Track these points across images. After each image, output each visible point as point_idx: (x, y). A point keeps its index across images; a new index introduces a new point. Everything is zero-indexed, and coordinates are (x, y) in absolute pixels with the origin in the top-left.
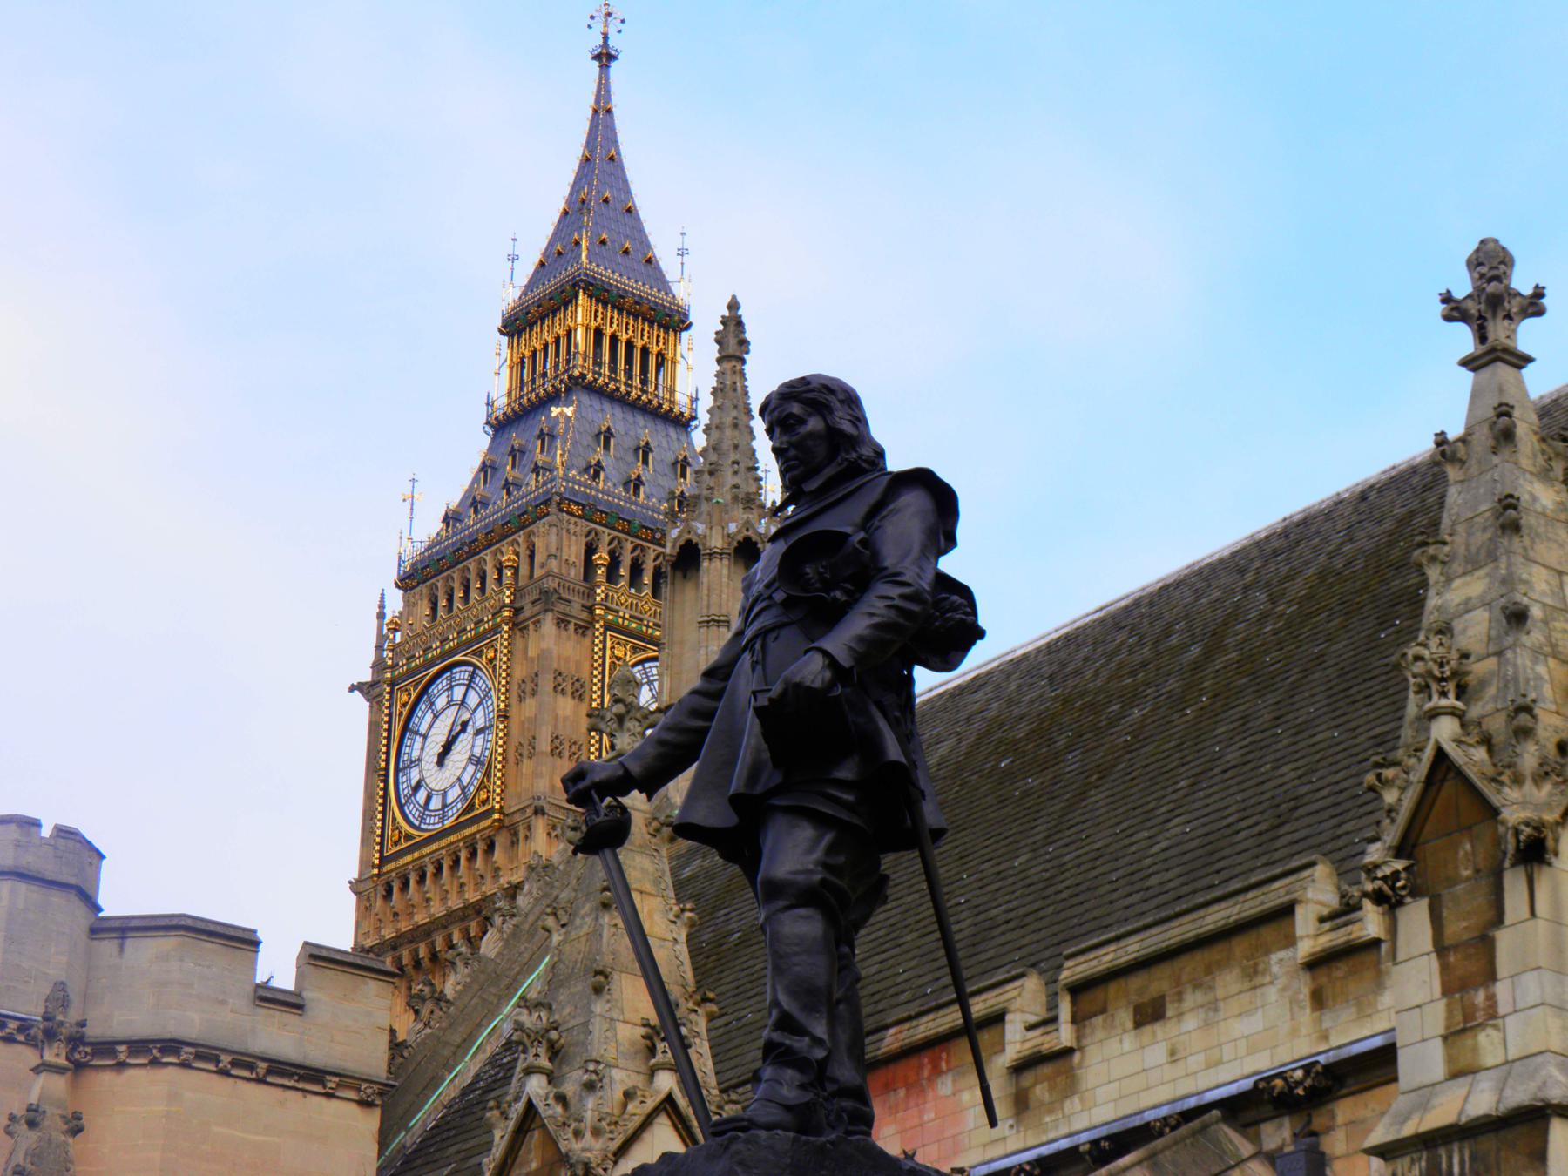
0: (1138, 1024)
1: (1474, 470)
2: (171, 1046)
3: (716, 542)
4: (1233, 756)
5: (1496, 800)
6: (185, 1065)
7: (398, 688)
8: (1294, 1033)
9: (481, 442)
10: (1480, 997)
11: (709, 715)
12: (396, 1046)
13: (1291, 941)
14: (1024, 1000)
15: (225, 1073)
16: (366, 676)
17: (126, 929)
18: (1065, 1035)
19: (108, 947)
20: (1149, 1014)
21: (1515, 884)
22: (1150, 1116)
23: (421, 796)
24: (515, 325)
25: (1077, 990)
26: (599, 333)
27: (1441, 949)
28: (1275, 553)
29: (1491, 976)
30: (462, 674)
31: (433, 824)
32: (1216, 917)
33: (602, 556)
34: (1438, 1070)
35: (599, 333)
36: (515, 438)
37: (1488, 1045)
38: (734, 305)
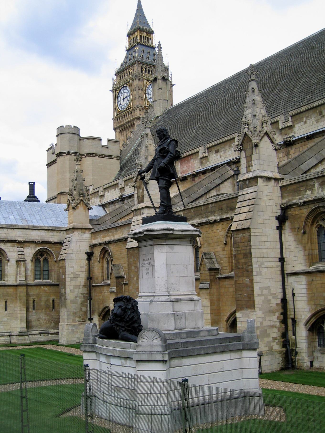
0: (216, 153)
1: (250, 95)
2: (92, 154)
3: (159, 77)
4: (230, 110)
5: (252, 139)
6: (94, 156)
7: (117, 90)
8: (235, 154)
9: (125, 53)
11: (153, 164)
12: (121, 151)
13: (235, 142)
14: (201, 149)
15: (99, 157)
16: (112, 89)
17: (84, 139)
18: (206, 154)
19: (82, 141)
20: (217, 151)
21: (254, 149)
22: (218, 165)
23: (121, 106)
24: (129, 35)
25: (208, 148)
26: (141, 36)
27: (246, 157)
28: (236, 79)
29: (252, 160)
30: (125, 88)
31: (123, 110)
32: (225, 139)
33: (144, 69)
34: (246, 172)
35: (141, 36)
36: (130, 52)
38: (159, 42)
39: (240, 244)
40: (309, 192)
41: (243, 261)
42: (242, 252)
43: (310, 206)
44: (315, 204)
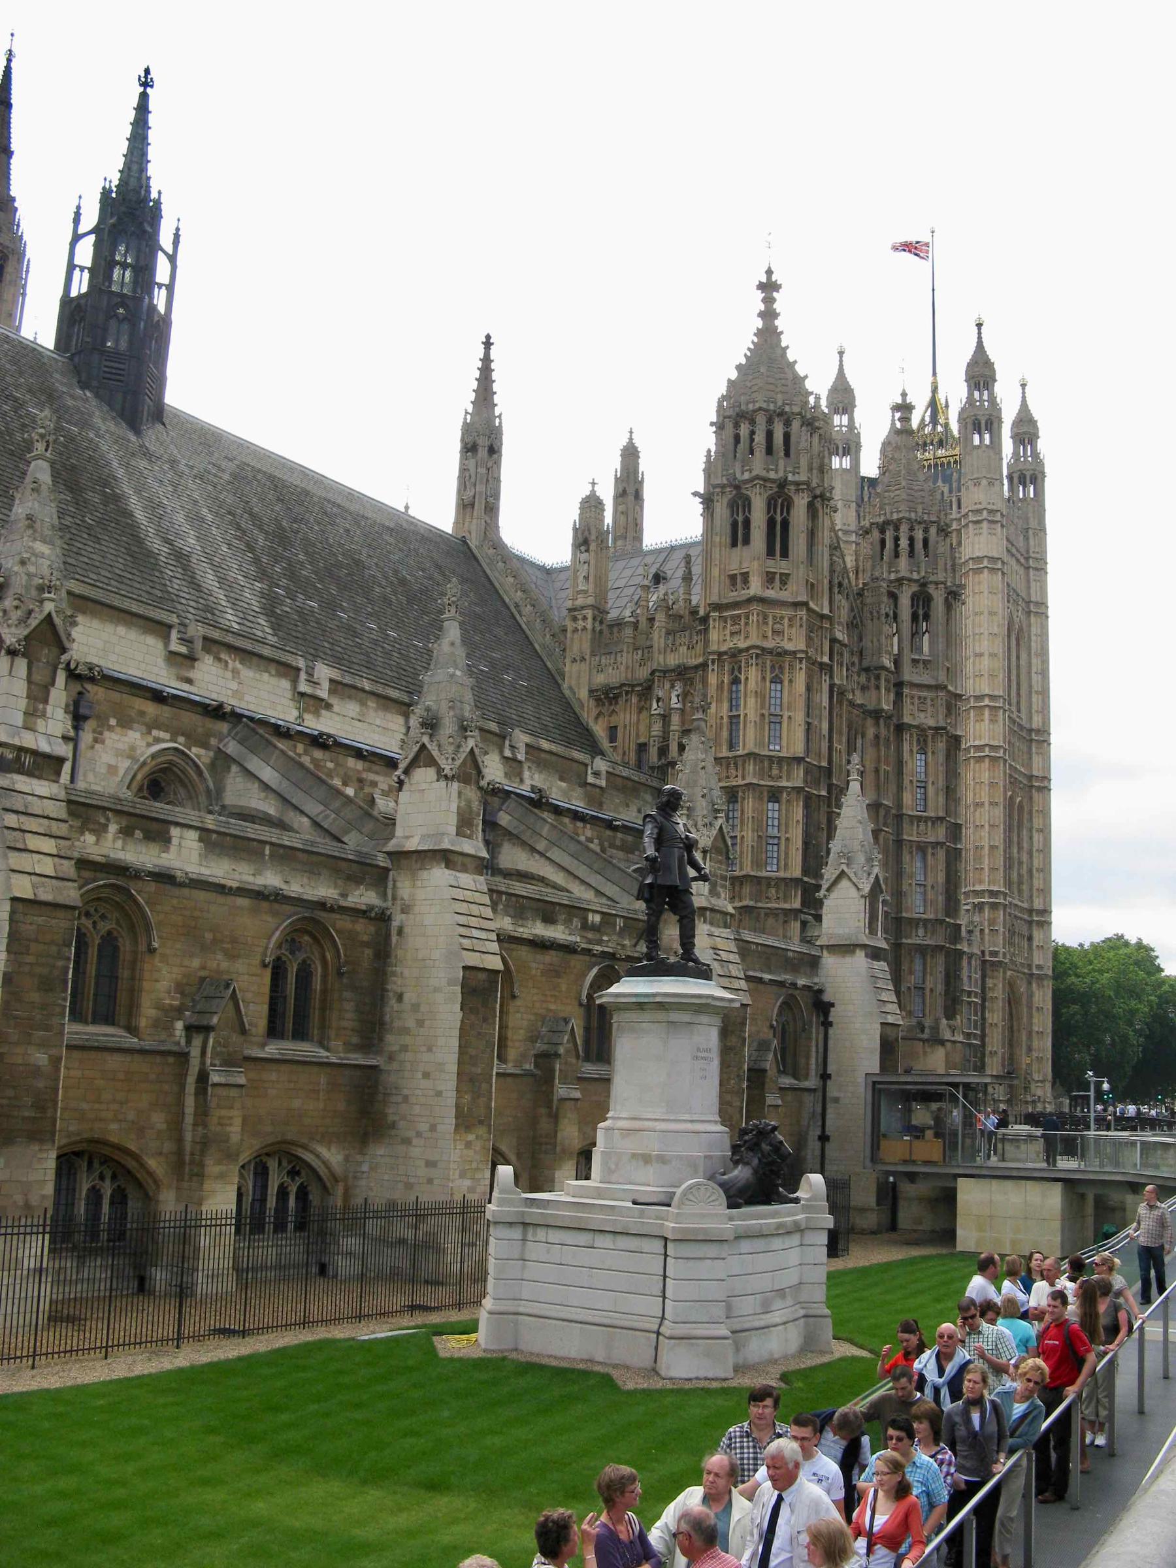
10: (41, 706)
29: (46, 702)
34: (20, 724)
37: (40, 724)
40: (90, 838)
41: (35, 997)
42: (38, 970)
44: (98, 875)
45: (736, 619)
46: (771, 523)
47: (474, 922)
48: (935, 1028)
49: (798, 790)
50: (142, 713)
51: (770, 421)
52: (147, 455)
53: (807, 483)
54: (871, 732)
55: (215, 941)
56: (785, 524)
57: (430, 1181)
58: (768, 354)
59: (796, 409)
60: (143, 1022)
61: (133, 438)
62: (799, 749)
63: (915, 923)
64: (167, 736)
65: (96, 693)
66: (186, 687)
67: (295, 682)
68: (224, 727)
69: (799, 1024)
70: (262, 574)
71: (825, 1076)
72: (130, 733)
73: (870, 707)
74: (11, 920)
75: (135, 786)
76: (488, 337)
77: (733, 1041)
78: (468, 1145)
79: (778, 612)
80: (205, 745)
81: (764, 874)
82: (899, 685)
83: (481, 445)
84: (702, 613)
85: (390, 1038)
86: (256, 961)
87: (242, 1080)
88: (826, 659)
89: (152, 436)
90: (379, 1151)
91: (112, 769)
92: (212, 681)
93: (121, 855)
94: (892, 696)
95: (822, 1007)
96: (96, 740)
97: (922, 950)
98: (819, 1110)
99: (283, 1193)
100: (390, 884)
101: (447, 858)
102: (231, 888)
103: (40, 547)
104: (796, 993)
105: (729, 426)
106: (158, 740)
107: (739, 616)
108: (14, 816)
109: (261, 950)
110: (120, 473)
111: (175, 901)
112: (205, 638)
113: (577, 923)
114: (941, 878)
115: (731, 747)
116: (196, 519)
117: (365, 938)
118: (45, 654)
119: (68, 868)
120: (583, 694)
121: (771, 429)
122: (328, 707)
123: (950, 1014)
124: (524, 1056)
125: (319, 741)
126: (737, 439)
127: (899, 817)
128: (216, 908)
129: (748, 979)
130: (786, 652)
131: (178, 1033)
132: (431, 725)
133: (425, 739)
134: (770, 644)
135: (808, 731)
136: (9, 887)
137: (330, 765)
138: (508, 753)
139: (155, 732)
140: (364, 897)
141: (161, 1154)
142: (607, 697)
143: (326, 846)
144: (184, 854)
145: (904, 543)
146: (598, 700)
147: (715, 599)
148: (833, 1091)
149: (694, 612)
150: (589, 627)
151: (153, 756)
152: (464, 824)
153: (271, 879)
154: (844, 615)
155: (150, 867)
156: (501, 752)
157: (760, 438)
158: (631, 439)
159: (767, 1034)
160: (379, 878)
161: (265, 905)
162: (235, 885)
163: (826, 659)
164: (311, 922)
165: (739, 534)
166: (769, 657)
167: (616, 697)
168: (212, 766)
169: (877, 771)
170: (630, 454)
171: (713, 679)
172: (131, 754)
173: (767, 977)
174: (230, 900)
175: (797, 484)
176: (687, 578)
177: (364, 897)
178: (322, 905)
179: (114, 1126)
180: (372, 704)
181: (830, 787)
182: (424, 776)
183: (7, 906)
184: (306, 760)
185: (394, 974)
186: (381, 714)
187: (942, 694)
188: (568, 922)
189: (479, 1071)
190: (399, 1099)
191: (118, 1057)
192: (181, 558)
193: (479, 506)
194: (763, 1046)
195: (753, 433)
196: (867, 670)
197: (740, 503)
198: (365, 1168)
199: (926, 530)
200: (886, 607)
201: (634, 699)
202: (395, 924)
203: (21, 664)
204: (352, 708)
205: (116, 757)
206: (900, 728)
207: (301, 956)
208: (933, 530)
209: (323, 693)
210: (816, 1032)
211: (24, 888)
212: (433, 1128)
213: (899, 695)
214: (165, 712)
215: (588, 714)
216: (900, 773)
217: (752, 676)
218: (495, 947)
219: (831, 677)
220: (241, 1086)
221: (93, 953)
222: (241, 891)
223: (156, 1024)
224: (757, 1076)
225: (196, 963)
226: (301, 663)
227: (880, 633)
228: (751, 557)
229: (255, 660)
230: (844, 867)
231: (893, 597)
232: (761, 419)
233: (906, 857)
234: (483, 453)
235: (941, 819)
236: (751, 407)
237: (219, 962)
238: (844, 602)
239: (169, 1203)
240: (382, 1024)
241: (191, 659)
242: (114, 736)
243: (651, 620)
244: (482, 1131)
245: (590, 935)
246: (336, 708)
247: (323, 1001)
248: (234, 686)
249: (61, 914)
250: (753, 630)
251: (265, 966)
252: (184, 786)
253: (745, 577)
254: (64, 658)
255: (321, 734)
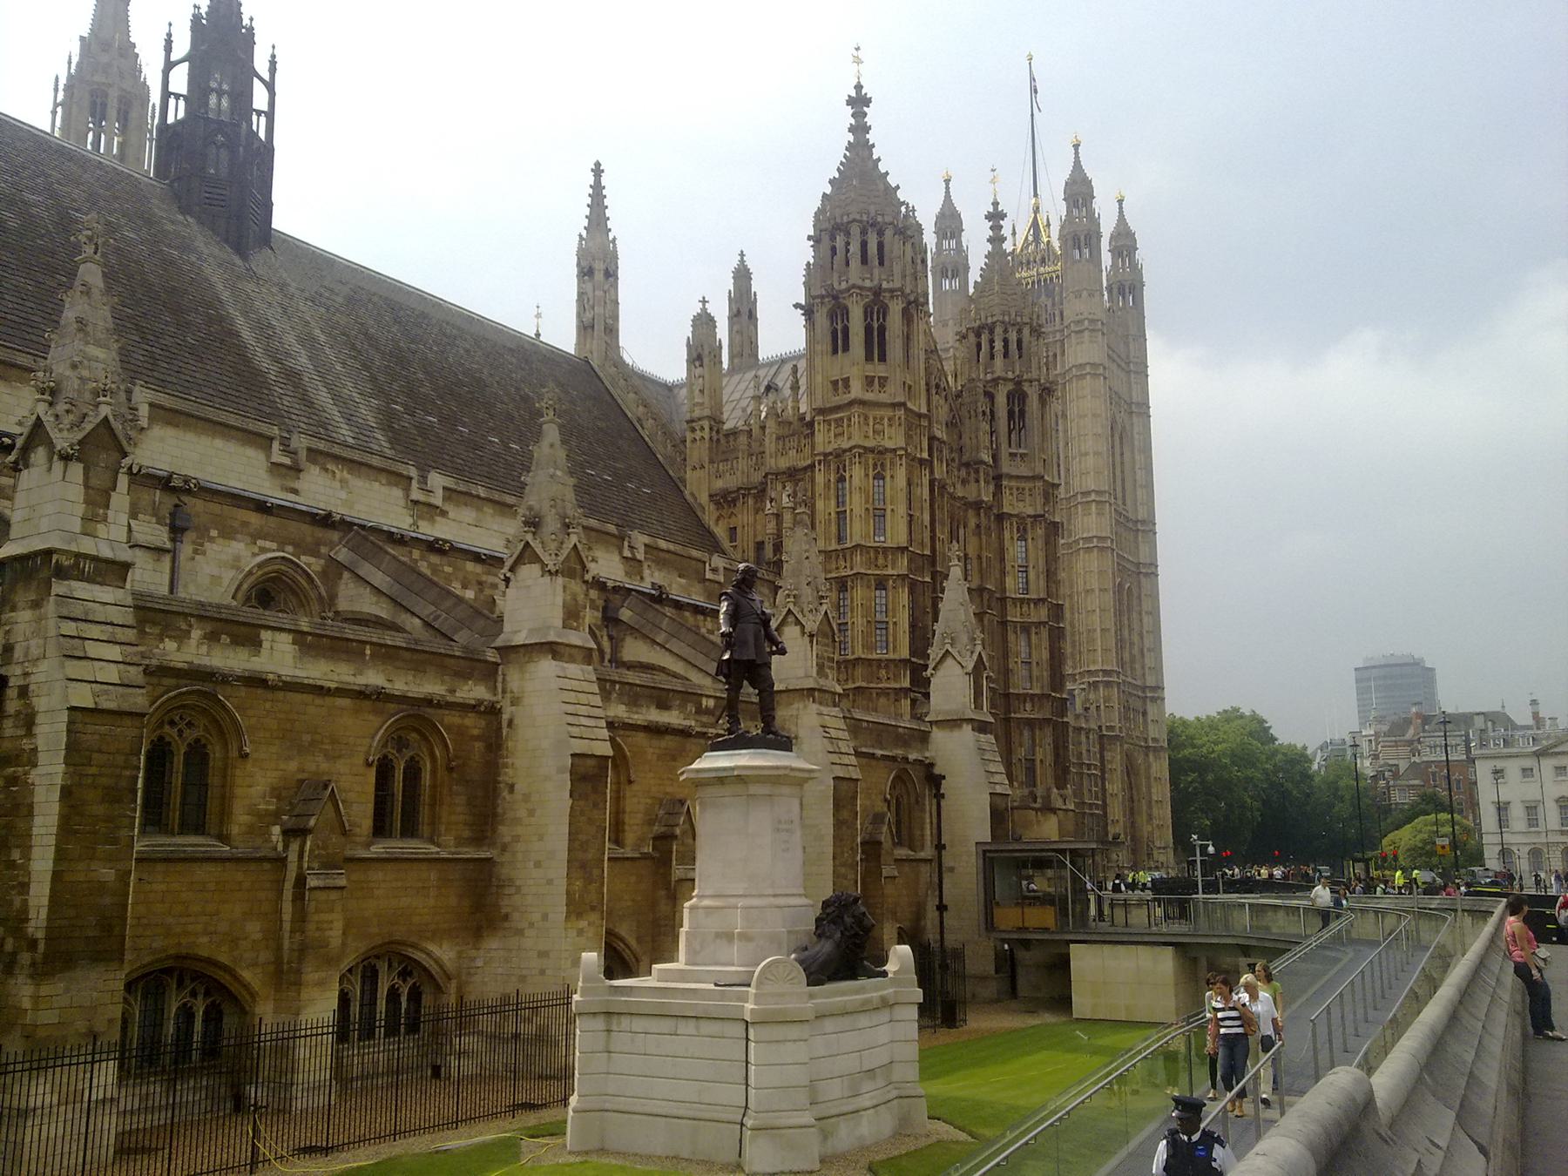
27: (86, 486)
29: (107, 507)
37: (101, 529)
39: (95, 755)
40: (170, 645)
41: (99, 810)
43: (168, 681)
45: (839, 422)
46: (868, 330)
47: (583, 710)
48: (1047, 798)
49: (903, 577)
50: (245, 524)
51: (864, 232)
52: (253, 276)
53: (901, 290)
54: (972, 522)
55: (313, 743)
56: (882, 330)
57: (542, 972)
58: (859, 167)
59: (888, 219)
60: (235, 830)
61: (238, 261)
62: (902, 540)
63: (1023, 698)
64: (274, 546)
65: (195, 505)
66: (292, 497)
67: (407, 490)
68: (335, 536)
69: (913, 800)
70: (379, 392)
71: (940, 847)
72: (234, 543)
73: (972, 497)
74: (68, 731)
75: (240, 595)
76: (598, 164)
77: (845, 814)
78: (580, 932)
79: (879, 413)
80: (317, 555)
81: (875, 656)
82: (998, 478)
83: (598, 268)
84: (808, 418)
85: (502, 829)
86: (360, 760)
87: (342, 882)
88: (925, 455)
89: (260, 261)
90: (492, 944)
91: (216, 580)
92: (320, 490)
93: (206, 661)
94: (992, 488)
95: (934, 781)
96: (196, 552)
97: (1030, 723)
98: (936, 880)
99: (393, 995)
100: (500, 679)
101: (553, 649)
102: (329, 689)
103: (94, 351)
104: (908, 767)
105: (826, 237)
106: (263, 550)
107: (842, 419)
108: (73, 624)
109: (364, 749)
110: (225, 295)
111: (268, 705)
112: (310, 450)
113: (691, 708)
114: (1045, 655)
115: (840, 539)
116: (308, 341)
117: (476, 732)
118: (104, 459)
119: (135, 674)
120: (704, 498)
121: (863, 236)
122: (444, 513)
123: (1061, 782)
124: (641, 840)
125: (435, 547)
126: (834, 250)
127: (1003, 600)
128: (314, 708)
129: (858, 754)
130: (887, 450)
131: (274, 838)
132: (534, 523)
133: (529, 537)
134: (870, 444)
135: (910, 523)
136: (66, 697)
137: (448, 569)
138: (627, 553)
139: (260, 542)
140: (473, 691)
141: (255, 964)
142: (725, 500)
143: (439, 646)
144: (278, 656)
145: (998, 345)
146: (718, 503)
147: (818, 404)
148: (947, 861)
149: (802, 418)
150: (707, 437)
151: (260, 566)
152: (571, 615)
153: (373, 678)
154: (942, 413)
155: (238, 672)
156: (621, 553)
157: (855, 248)
158: (742, 261)
159: (881, 807)
160: (489, 673)
161: (367, 704)
162: (333, 685)
163: (925, 455)
164: (416, 718)
165: (839, 341)
166: (871, 456)
167: (734, 501)
168: (324, 574)
169: (979, 557)
170: (742, 276)
171: (820, 478)
172: (235, 563)
173: (879, 752)
174: (329, 700)
175: (892, 291)
176: (795, 387)
177: (473, 691)
178: (428, 701)
179: (205, 939)
180: (488, 510)
181: (934, 575)
182: (529, 572)
183: (65, 717)
184: (424, 567)
185: (506, 766)
186: (498, 519)
187: (1039, 484)
188: (682, 708)
189: (590, 856)
190: (512, 890)
191: (210, 867)
192: (292, 377)
193: (599, 327)
194: (878, 819)
195: (848, 244)
196: (967, 465)
197: (839, 313)
198: (479, 963)
199: (1020, 331)
200: (983, 404)
201: (751, 501)
202: (505, 717)
203: (77, 470)
204: (467, 514)
205: (219, 568)
206: (1001, 518)
207: (408, 754)
208: (1026, 331)
209: (437, 500)
210: (929, 804)
211: (83, 697)
212: (545, 917)
213: (998, 487)
214: (272, 522)
215: (709, 516)
216: (1002, 560)
217: (857, 474)
218: (605, 733)
219: (932, 472)
220: (342, 888)
221: (179, 762)
222: (341, 692)
223: (250, 830)
224: (872, 848)
225: (293, 766)
226: (413, 472)
227: (977, 430)
228: (853, 365)
229: (364, 469)
230: (948, 647)
231: (990, 396)
232: (855, 230)
233: (1011, 637)
234: (599, 276)
235: (1043, 600)
236: (845, 219)
237: (317, 764)
238: (942, 402)
239: (266, 1013)
240: (495, 815)
241: (296, 470)
242: (215, 547)
243: (763, 428)
244: (594, 917)
245: (705, 719)
246: (451, 515)
247: (433, 797)
248: (343, 495)
249: (128, 721)
250: (855, 430)
251: (369, 765)
252: (294, 593)
253: (846, 381)
254: (126, 462)
255: (437, 540)
